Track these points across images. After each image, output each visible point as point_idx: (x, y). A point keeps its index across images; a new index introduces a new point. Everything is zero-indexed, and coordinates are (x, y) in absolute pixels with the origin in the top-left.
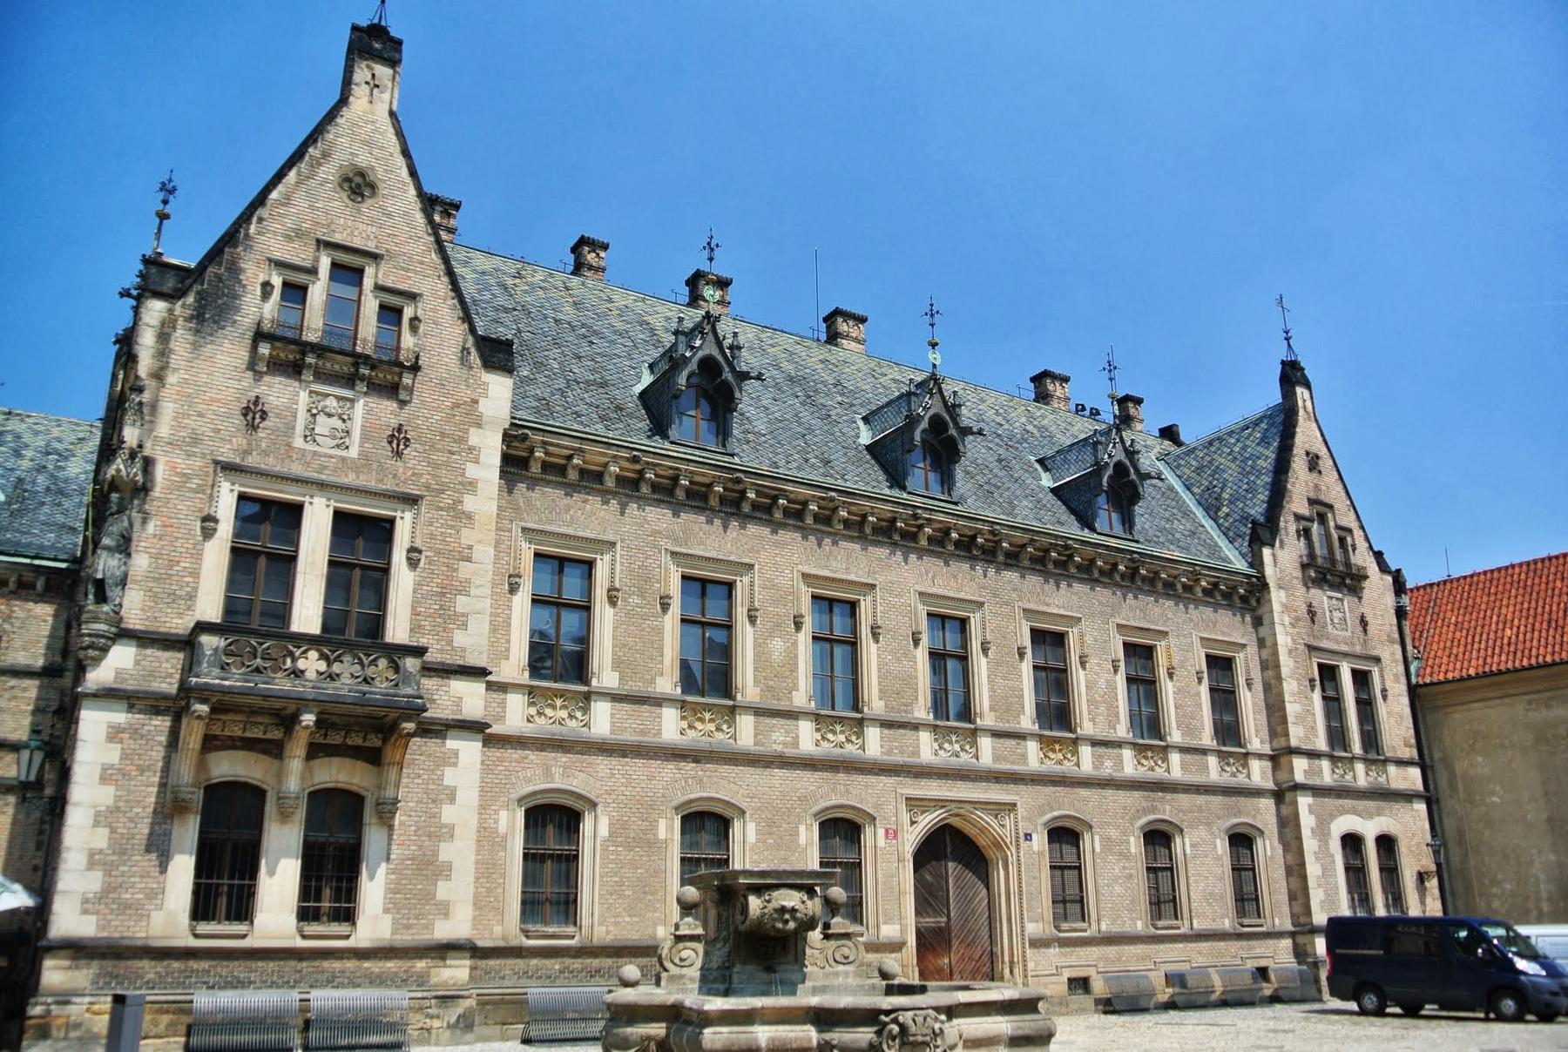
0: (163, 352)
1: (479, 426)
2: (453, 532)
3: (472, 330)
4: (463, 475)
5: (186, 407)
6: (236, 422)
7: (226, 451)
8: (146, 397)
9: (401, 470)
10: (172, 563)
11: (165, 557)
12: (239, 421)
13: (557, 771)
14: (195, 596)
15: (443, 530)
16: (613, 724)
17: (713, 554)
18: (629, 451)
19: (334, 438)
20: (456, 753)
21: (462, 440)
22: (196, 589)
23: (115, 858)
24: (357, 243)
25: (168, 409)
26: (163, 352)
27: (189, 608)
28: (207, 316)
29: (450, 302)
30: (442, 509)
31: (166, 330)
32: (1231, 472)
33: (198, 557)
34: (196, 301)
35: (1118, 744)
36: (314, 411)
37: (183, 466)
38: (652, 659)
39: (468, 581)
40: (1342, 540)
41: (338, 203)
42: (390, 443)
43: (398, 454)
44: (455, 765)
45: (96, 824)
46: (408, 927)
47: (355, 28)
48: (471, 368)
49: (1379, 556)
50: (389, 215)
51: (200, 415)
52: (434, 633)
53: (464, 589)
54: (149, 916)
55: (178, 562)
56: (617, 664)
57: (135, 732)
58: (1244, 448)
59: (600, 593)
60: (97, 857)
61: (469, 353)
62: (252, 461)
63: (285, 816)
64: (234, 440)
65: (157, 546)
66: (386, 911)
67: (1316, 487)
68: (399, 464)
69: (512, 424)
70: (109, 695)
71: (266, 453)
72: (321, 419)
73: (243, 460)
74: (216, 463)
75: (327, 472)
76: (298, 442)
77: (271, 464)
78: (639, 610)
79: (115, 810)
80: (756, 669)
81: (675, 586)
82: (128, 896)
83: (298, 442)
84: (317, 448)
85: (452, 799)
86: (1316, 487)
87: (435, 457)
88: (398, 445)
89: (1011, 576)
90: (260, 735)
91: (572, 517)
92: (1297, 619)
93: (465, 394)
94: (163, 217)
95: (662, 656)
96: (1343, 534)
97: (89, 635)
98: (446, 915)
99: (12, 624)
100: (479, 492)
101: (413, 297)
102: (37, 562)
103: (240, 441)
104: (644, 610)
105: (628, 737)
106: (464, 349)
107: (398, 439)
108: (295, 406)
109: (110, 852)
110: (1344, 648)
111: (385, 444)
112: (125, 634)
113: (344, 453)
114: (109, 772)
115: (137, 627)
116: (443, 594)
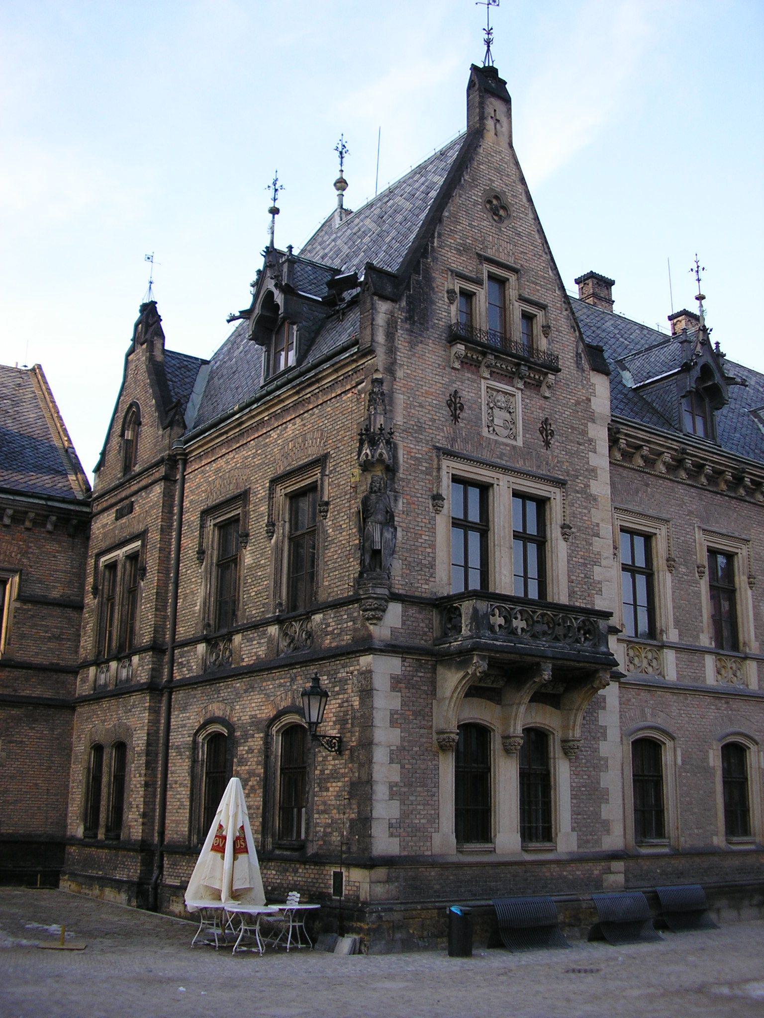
0: (391, 350)
1: (593, 421)
2: (584, 511)
3: (581, 338)
4: (588, 463)
5: (411, 399)
6: (444, 412)
7: (440, 438)
8: (385, 388)
9: (550, 457)
10: (418, 536)
11: (412, 530)
12: (446, 412)
14: (435, 565)
15: (580, 510)
16: (678, 674)
17: (724, 531)
18: (678, 444)
19: (506, 428)
21: (584, 433)
22: (434, 559)
23: (406, 790)
24: (502, 258)
25: (400, 399)
26: (391, 350)
27: (431, 576)
28: (416, 318)
29: (565, 313)
30: (578, 492)
31: (391, 330)
33: (433, 530)
34: (407, 303)
36: (492, 405)
37: (414, 451)
38: (696, 619)
39: (599, 553)
41: (486, 223)
42: (542, 433)
43: (547, 444)
44: (604, 708)
45: (392, 761)
46: (588, 841)
47: (474, 68)
48: (583, 371)
50: (519, 235)
51: (421, 406)
52: (583, 597)
53: (596, 563)
54: (431, 837)
55: (421, 535)
56: (677, 623)
57: (410, 686)
59: (660, 562)
60: (394, 789)
61: (581, 358)
62: (457, 448)
63: (507, 751)
64: (445, 429)
65: (406, 521)
66: (573, 829)
68: (549, 452)
69: (612, 420)
70: (391, 649)
71: (465, 441)
72: (496, 411)
73: (452, 446)
74: (438, 449)
75: (505, 458)
77: (468, 449)
78: (686, 577)
80: (756, 628)
81: (702, 557)
82: (417, 821)
83: (485, 432)
84: (496, 438)
85: (604, 736)
87: (569, 447)
88: (547, 436)
90: (490, 685)
91: (641, 498)
93: (582, 394)
94: (274, 211)
95: (701, 616)
97: (375, 598)
98: (608, 832)
100: (599, 478)
101: (543, 307)
102: (50, 503)
103: (448, 429)
104: (689, 578)
105: (687, 682)
106: (577, 353)
107: (546, 431)
108: (479, 400)
109: (402, 784)
111: (538, 434)
112: (395, 597)
113: (514, 443)
114: (395, 716)
115: (401, 592)
116: (585, 565)
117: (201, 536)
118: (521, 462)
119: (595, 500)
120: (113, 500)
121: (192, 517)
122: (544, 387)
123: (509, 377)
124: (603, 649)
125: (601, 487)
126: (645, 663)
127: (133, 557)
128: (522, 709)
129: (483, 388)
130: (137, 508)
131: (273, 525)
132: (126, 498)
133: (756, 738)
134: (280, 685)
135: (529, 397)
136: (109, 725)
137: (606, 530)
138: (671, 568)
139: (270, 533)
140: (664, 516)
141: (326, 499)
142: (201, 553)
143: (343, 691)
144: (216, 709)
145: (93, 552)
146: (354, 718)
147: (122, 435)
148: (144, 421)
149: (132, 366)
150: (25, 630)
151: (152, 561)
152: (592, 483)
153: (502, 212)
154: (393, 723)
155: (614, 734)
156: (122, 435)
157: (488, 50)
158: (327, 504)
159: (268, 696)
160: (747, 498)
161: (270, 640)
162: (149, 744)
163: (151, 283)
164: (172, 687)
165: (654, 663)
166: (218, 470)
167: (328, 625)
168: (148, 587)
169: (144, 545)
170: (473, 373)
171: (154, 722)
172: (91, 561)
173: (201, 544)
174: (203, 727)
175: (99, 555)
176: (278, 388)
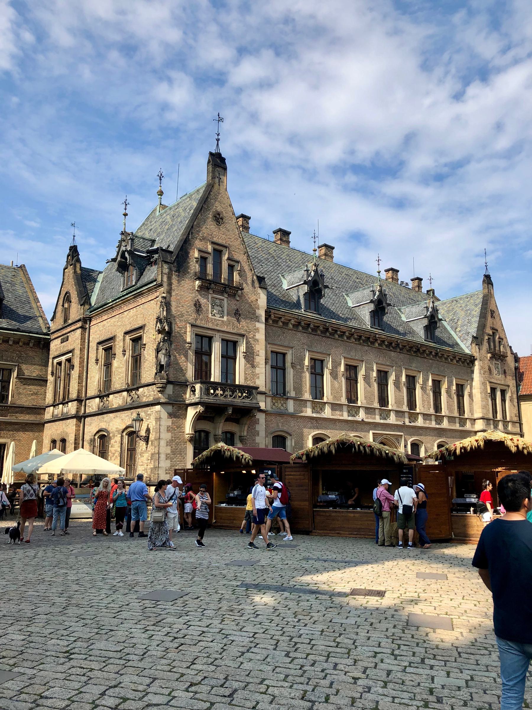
13: (280, 425)
20: (258, 419)
21: (254, 314)
24: (220, 241)
32: (462, 314)
35: (431, 415)
40: (499, 342)
44: (258, 423)
47: (211, 154)
49: (511, 347)
56: (295, 389)
58: (466, 305)
59: (288, 364)
67: (493, 322)
71: (201, 320)
76: (210, 315)
79: (171, 441)
83: (210, 315)
85: (258, 435)
86: (493, 322)
89: (402, 356)
92: (485, 372)
96: (500, 340)
99: (21, 359)
101: (238, 262)
103: (194, 315)
110: (499, 382)
117: (97, 353)
118: (226, 327)
119: (258, 341)
120: (59, 334)
121: (93, 345)
122: (237, 296)
123: (222, 293)
124: (254, 401)
125: (261, 336)
126: (280, 405)
127: (69, 360)
128: (221, 424)
129: (210, 296)
130: (69, 338)
131: (125, 351)
132: (66, 334)
133: (329, 435)
134: (127, 416)
135: (230, 301)
136: (59, 432)
137: (262, 353)
138: (292, 367)
139: (124, 355)
140: (291, 345)
141: (144, 343)
142: (97, 360)
143: (149, 418)
144: (103, 426)
145: (51, 356)
146: (153, 429)
147: (63, 306)
148: (72, 300)
149: (66, 274)
150: (21, 391)
151: (76, 362)
152: (257, 334)
153: (220, 220)
154: (168, 431)
155: (262, 433)
156: (63, 306)
157: (218, 144)
158: (145, 345)
159: (122, 420)
160: (331, 336)
161: (124, 398)
162: (75, 440)
163: (74, 236)
164: (85, 416)
165: (284, 405)
166: (104, 326)
167: (145, 393)
168: (75, 374)
169: (73, 355)
170: (205, 292)
171: (78, 431)
172: (51, 361)
173: (97, 357)
174: (98, 432)
175: (54, 358)
176: (127, 294)
